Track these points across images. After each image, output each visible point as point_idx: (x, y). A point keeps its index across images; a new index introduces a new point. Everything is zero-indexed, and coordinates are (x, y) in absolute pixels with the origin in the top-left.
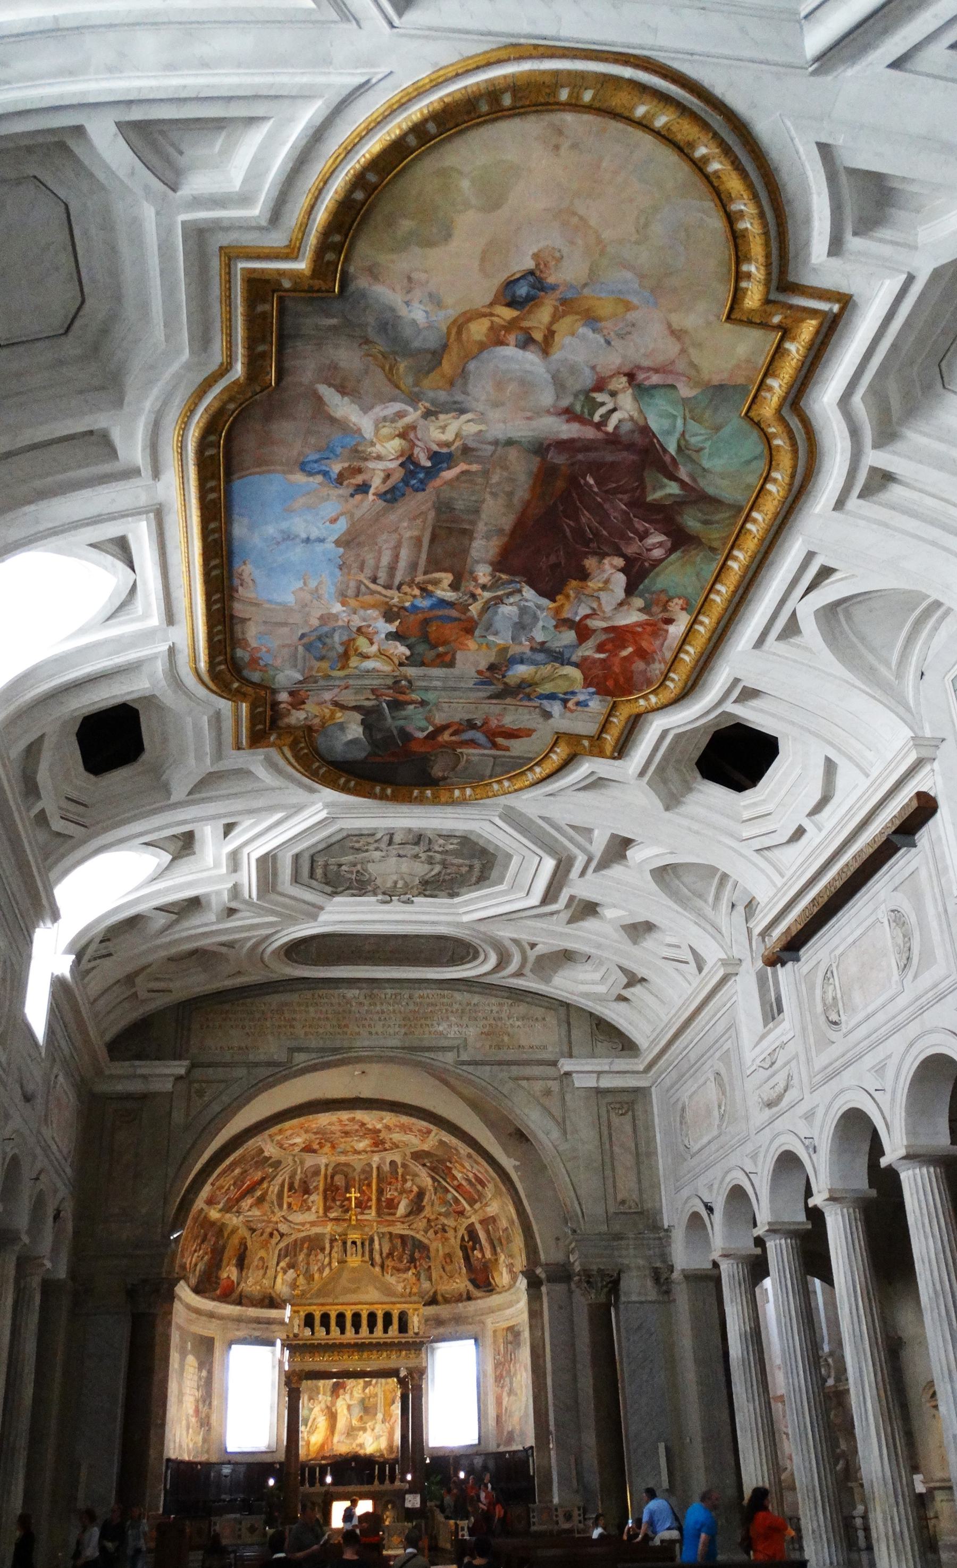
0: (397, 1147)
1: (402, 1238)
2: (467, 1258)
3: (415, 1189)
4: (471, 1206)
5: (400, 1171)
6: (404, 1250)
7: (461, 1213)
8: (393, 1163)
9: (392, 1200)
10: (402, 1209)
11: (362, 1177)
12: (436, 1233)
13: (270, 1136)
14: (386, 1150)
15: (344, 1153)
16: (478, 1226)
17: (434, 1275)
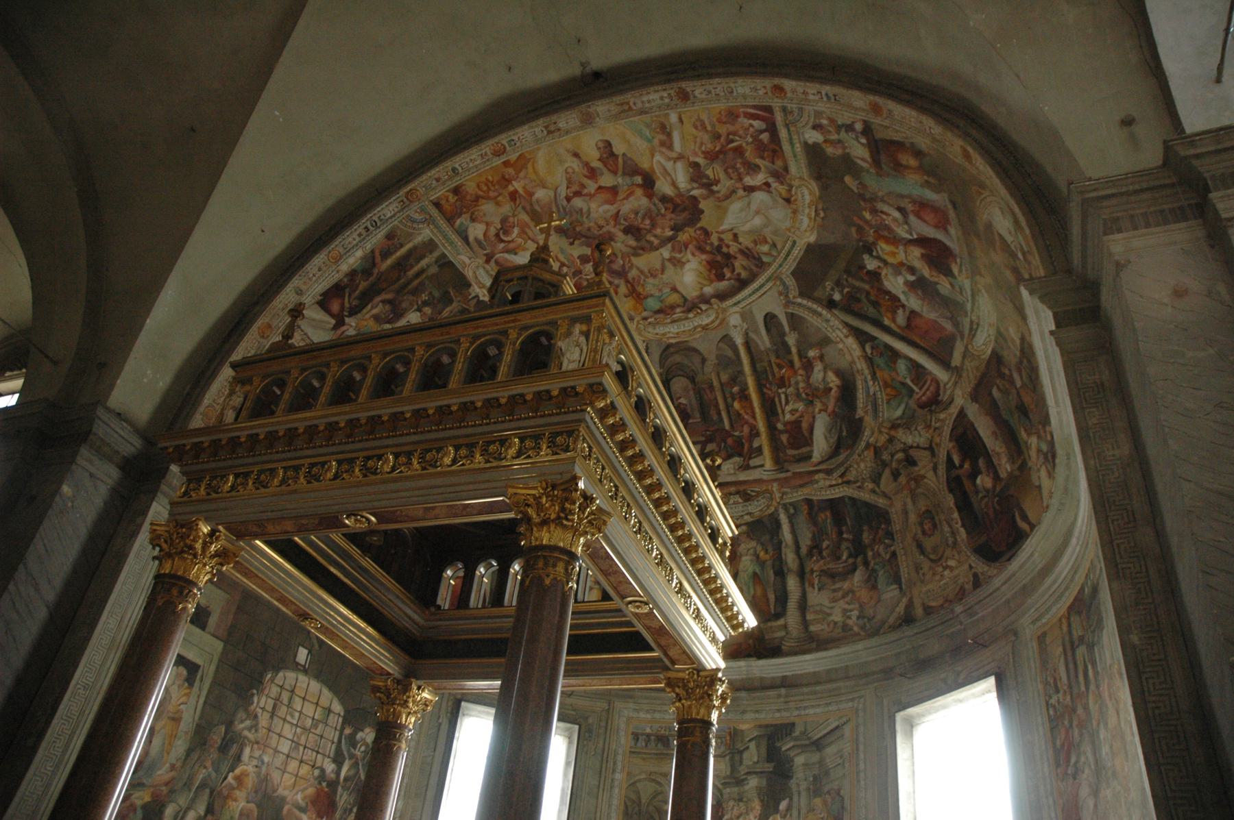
0: (761, 265)
1: (833, 505)
2: (964, 504)
3: (834, 381)
4: (945, 364)
5: (791, 340)
6: (840, 533)
7: (934, 403)
8: (770, 319)
9: (797, 424)
10: (821, 444)
11: (725, 377)
12: (896, 475)
13: (437, 205)
14: (743, 284)
15: (665, 311)
16: (973, 411)
17: (904, 572)
